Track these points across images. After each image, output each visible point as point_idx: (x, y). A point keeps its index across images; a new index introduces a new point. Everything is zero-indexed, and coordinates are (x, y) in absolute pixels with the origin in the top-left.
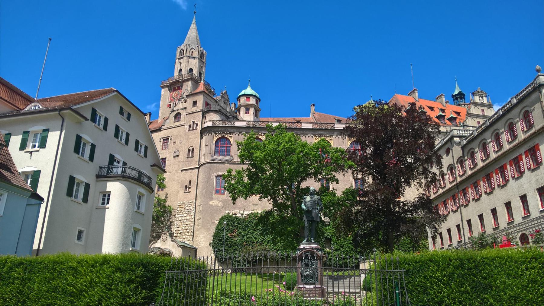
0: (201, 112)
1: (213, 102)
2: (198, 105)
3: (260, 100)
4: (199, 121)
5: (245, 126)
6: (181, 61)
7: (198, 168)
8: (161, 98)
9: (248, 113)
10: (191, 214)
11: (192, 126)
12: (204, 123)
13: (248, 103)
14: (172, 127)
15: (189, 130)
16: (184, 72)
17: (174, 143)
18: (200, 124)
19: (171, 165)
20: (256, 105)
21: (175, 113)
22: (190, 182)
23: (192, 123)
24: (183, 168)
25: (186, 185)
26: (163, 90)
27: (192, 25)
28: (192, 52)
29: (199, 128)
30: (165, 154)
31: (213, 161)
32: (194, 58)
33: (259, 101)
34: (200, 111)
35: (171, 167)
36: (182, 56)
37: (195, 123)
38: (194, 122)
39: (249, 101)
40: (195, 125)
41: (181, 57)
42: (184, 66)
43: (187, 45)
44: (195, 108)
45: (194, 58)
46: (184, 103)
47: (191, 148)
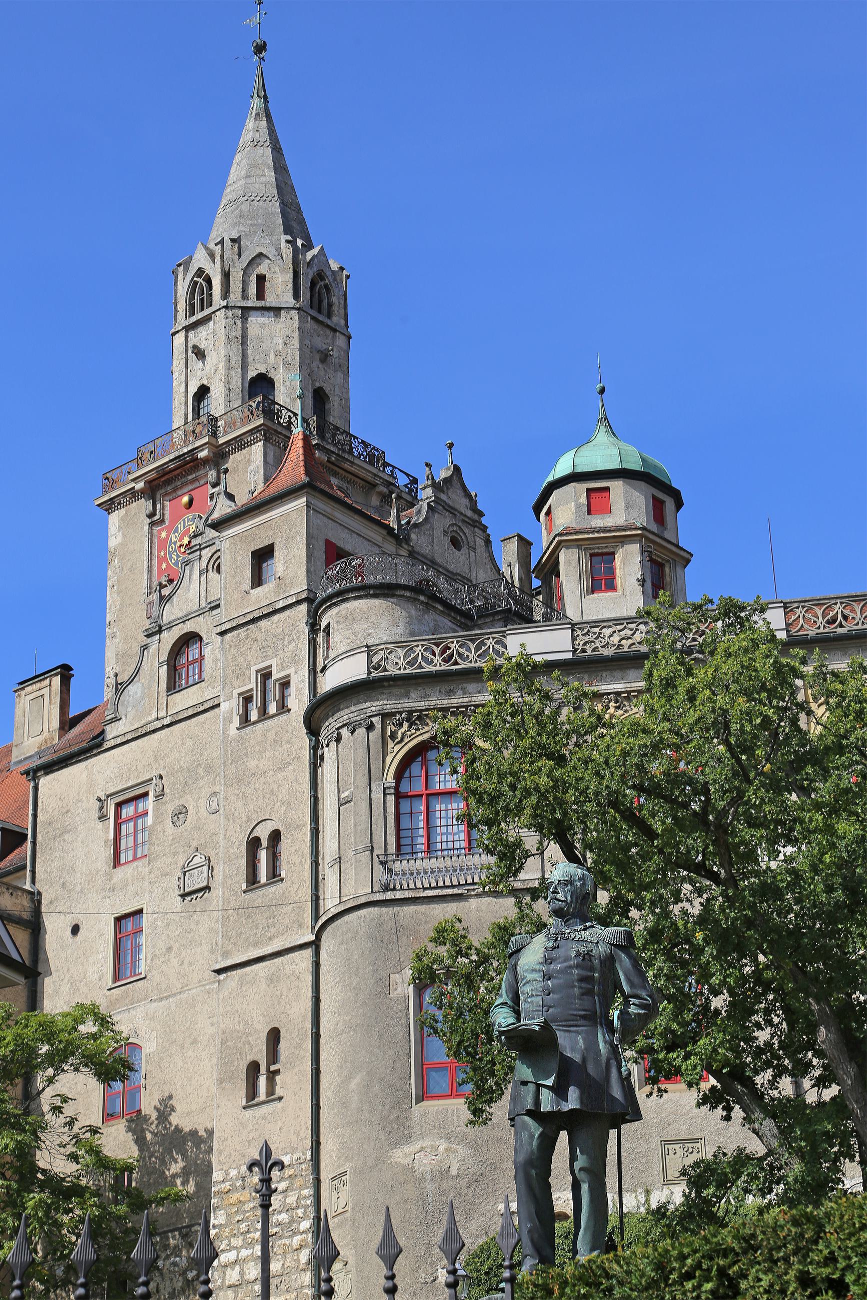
0: (304, 607)
1: (378, 539)
4: (295, 660)
5: (569, 656)
6: (200, 337)
7: (316, 945)
8: (109, 573)
9: (611, 586)
10: (296, 1240)
12: (324, 669)
13: (598, 521)
14: (158, 724)
15: (245, 720)
17: (181, 813)
19: (169, 949)
20: (654, 527)
21: (169, 638)
22: (274, 1036)
25: (250, 1058)
26: (114, 519)
27: (250, 124)
28: (261, 279)
30: (131, 889)
31: (389, 895)
32: (276, 311)
34: (299, 602)
35: (175, 962)
36: (207, 312)
39: (606, 509)
41: (199, 316)
42: (222, 366)
43: (228, 243)
45: (276, 311)
46: (212, 575)
47: (264, 833)
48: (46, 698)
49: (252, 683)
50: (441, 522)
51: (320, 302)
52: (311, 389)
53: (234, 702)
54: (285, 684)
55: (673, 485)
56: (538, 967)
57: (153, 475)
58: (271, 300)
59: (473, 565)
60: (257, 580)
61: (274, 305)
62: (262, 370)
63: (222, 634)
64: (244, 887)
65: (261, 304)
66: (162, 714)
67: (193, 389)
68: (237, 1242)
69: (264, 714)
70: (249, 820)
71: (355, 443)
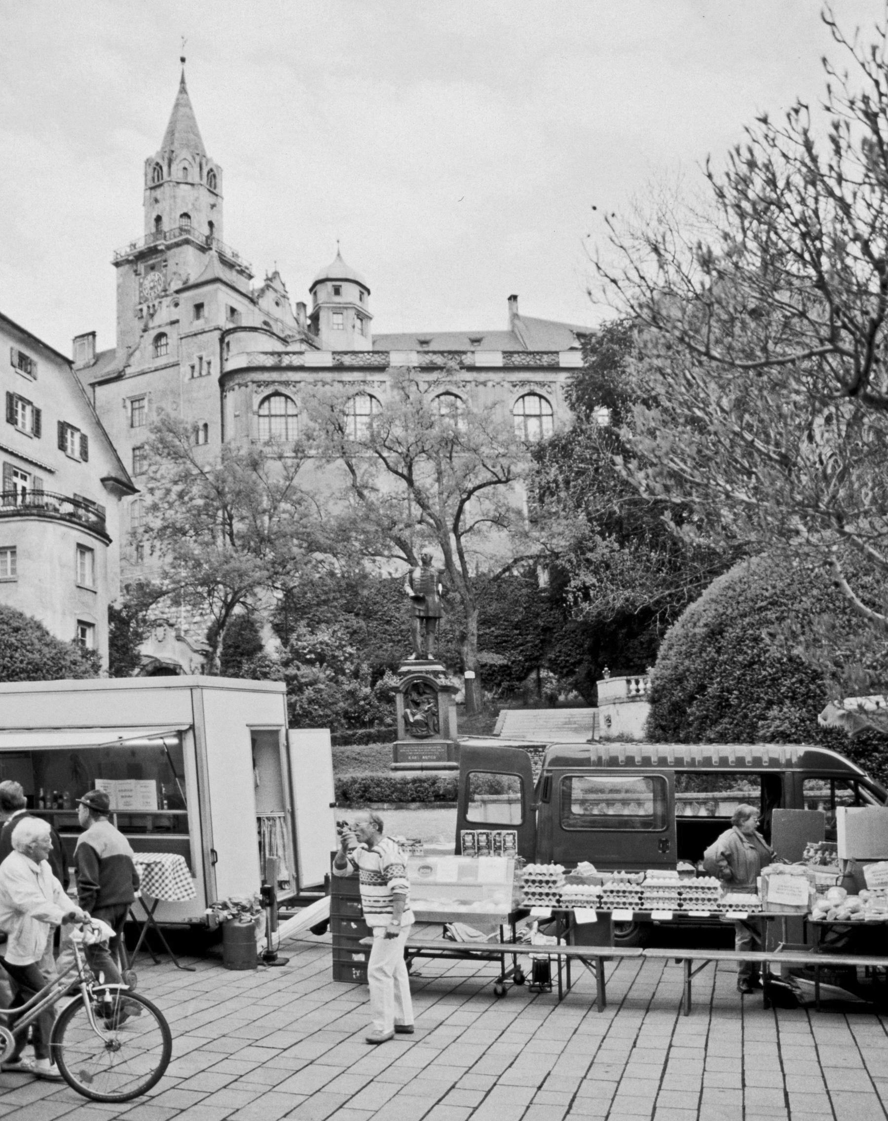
2: (206, 311)
11: (197, 368)
18: (216, 362)
21: (153, 333)
23: (196, 362)
29: (216, 374)
37: (205, 359)
38: (201, 359)
40: (205, 365)
41: (157, 183)
44: (201, 321)
45: (192, 185)
46: (173, 308)
47: (201, 424)
54: (209, 363)
62: (185, 211)
67: (154, 216)
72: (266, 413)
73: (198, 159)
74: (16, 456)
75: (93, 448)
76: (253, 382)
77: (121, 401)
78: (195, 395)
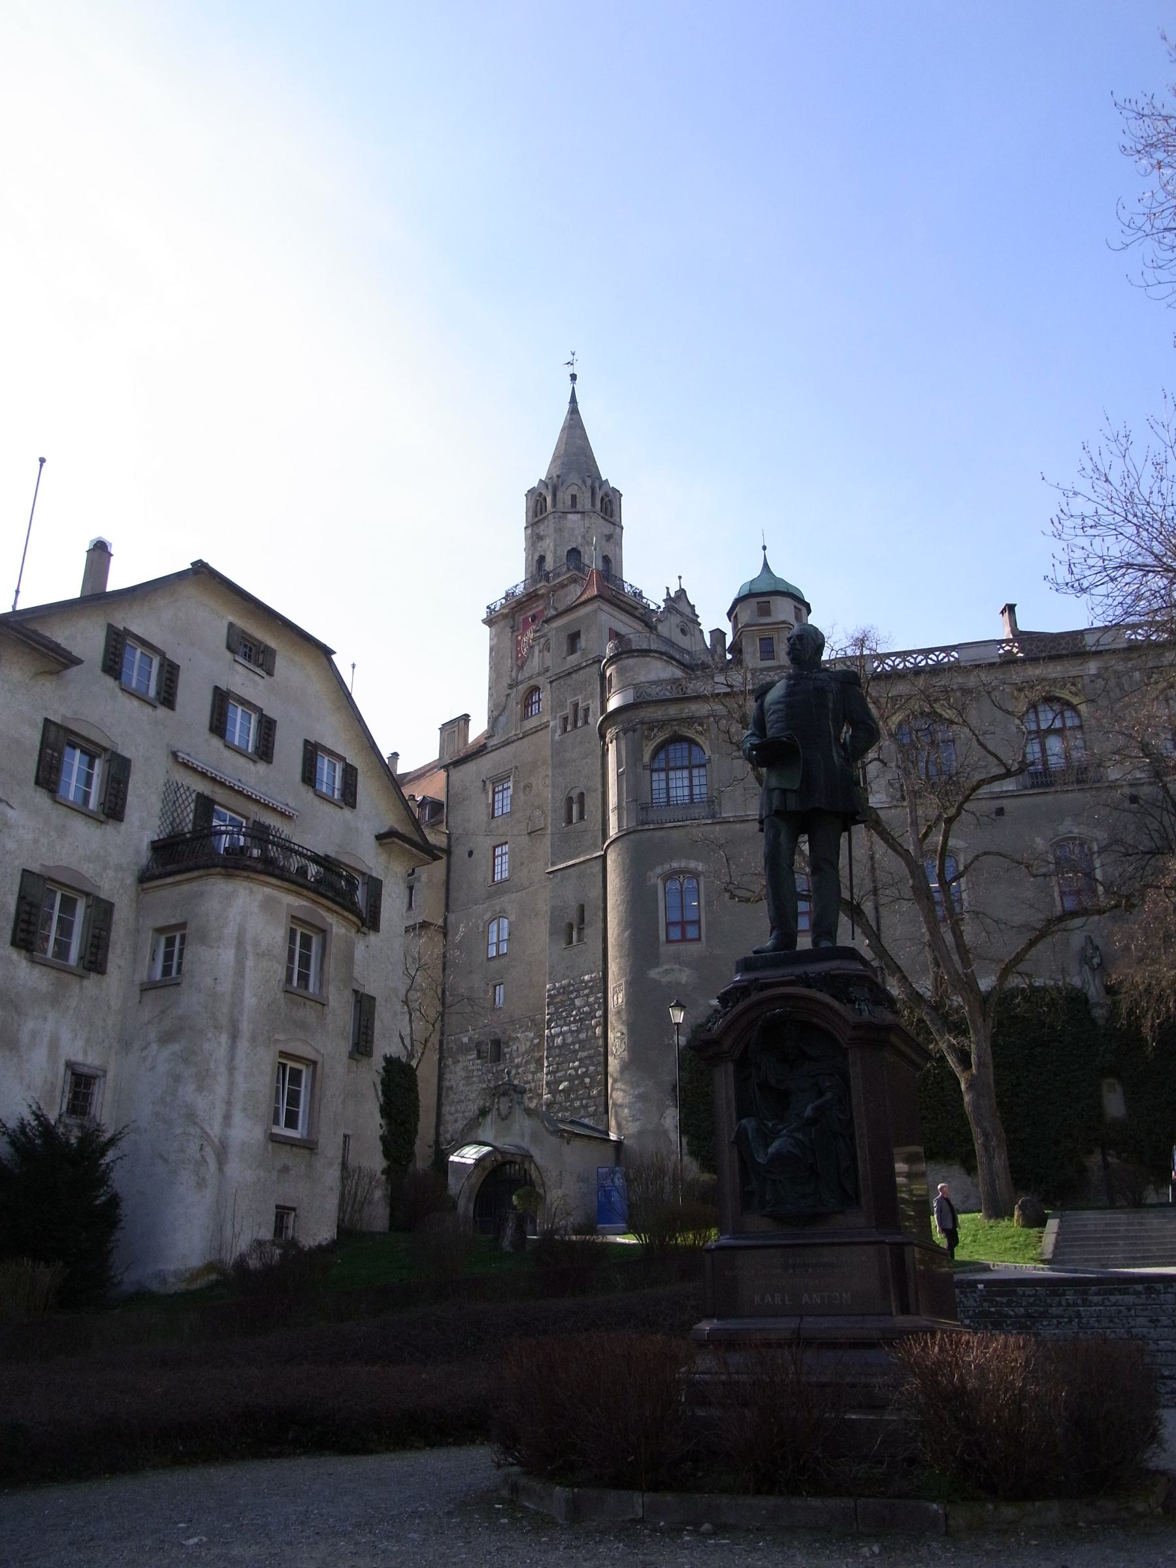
2: (583, 643)
3: (808, 606)
4: (592, 696)
11: (570, 720)
14: (516, 738)
16: (552, 563)
18: (595, 705)
21: (522, 688)
22: (582, 909)
24: (553, 864)
31: (646, 827)
33: (804, 609)
36: (544, 515)
41: (540, 517)
47: (575, 794)
48: (456, 732)
49: (568, 710)
50: (675, 620)
51: (606, 509)
52: (601, 556)
53: (558, 721)
54: (587, 710)
55: (806, 600)
56: (782, 700)
57: (514, 605)
58: (579, 508)
59: (693, 645)
60: (572, 649)
61: (581, 510)
62: (574, 546)
63: (551, 682)
64: (564, 825)
65: (575, 510)
66: (518, 732)
67: (536, 558)
68: (561, 1022)
69: (575, 726)
70: (566, 787)
71: (626, 585)
72: (663, 765)
73: (589, 482)
74: (222, 784)
75: (367, 788)
76: (642, 723)
77: (481, 784)
78: (568, 755)
